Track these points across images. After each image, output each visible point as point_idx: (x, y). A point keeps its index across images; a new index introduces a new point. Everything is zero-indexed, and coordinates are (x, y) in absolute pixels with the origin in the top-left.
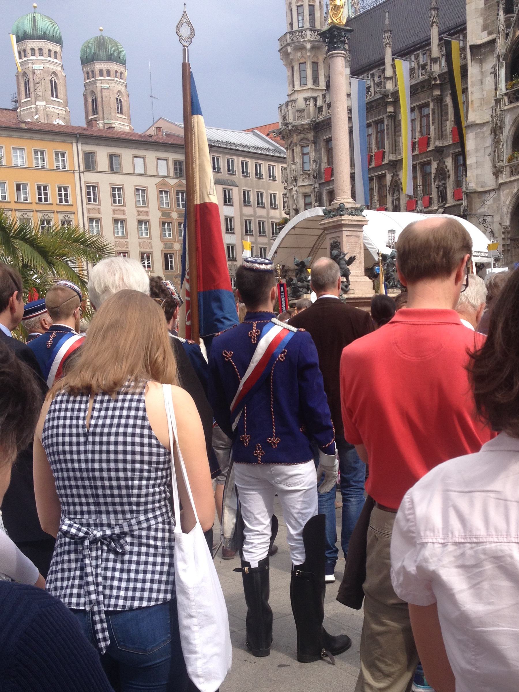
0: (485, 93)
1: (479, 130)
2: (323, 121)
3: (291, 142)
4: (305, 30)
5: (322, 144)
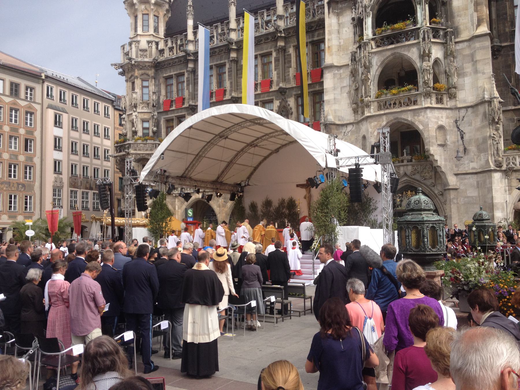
0: (342, 41)
1: (336, 72)
2: (164, 61)
3: (132, 76)
5: (162, 80)
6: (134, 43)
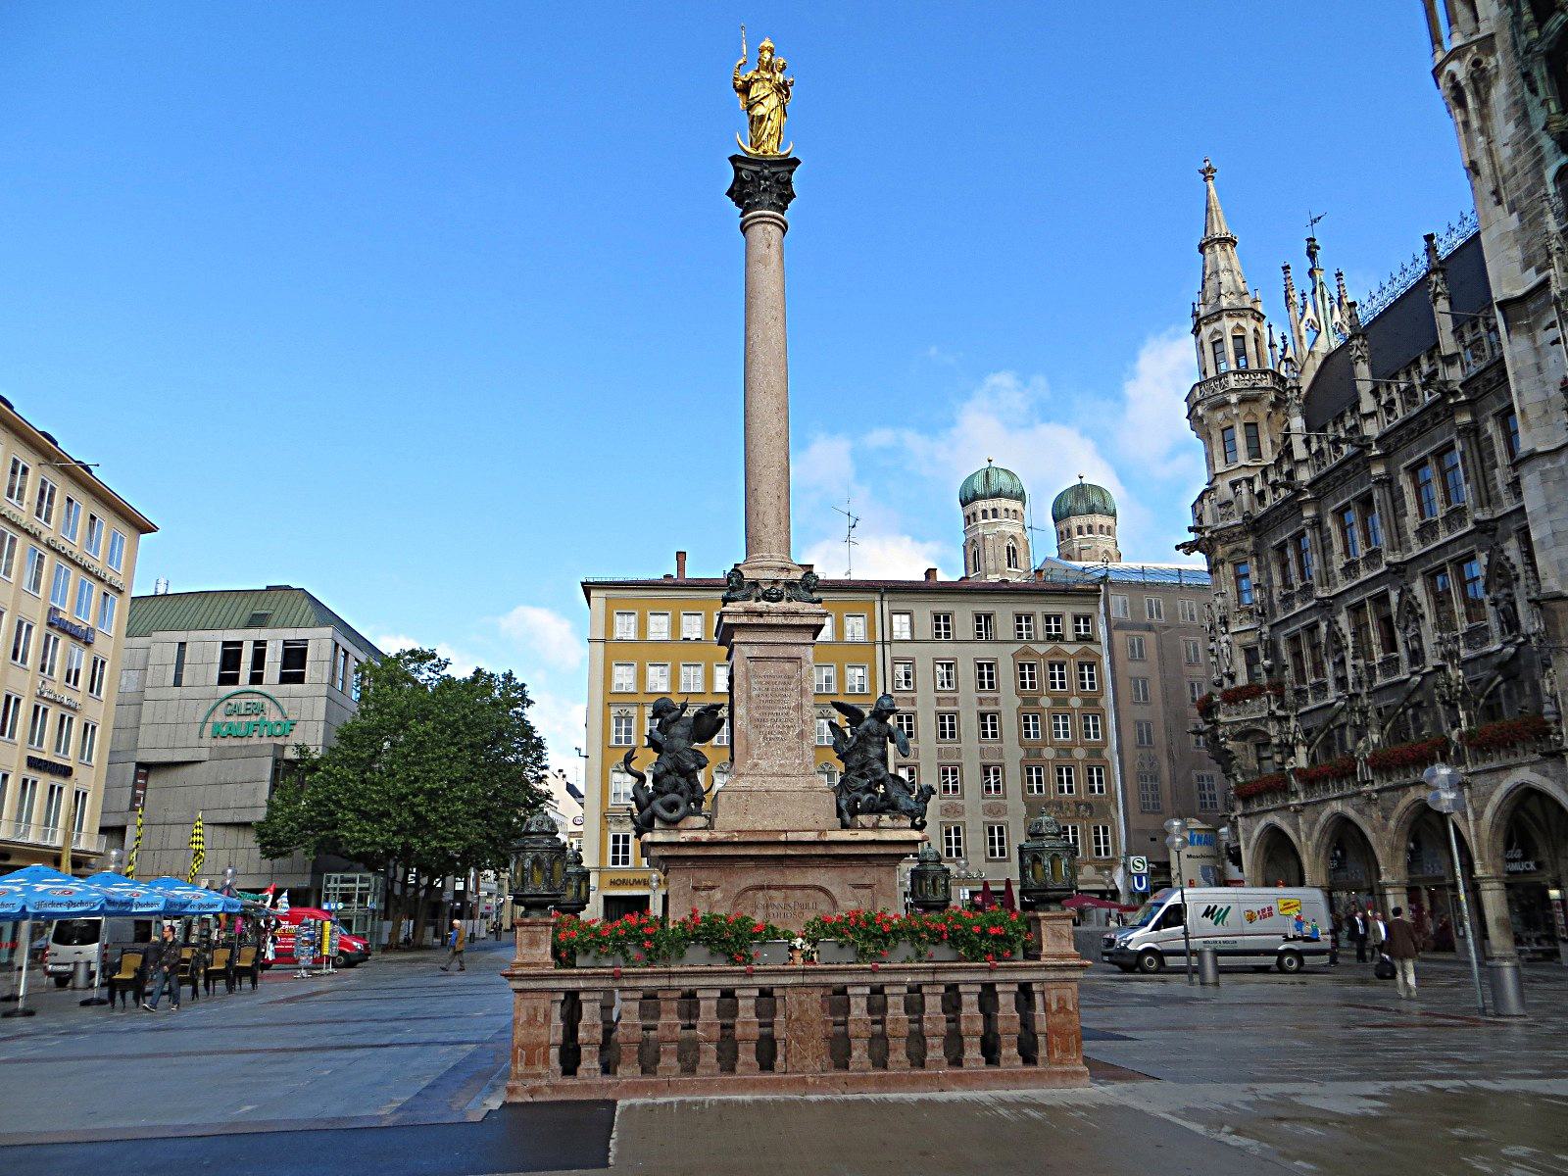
1: (1549, 466)
2: (1265, 515)
5: (1271, 555)
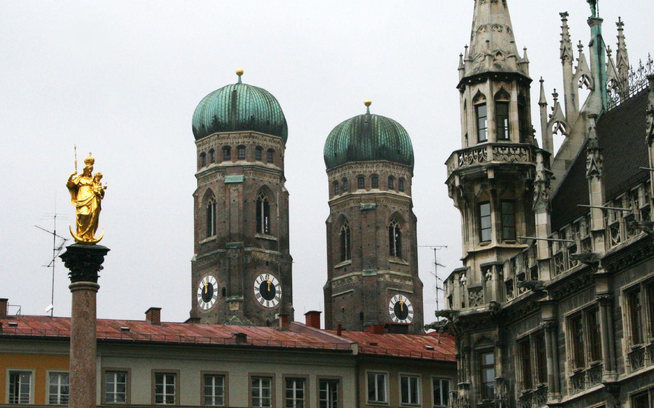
4: (485, 147)
5: (514, 348)
6: (457, 277)
